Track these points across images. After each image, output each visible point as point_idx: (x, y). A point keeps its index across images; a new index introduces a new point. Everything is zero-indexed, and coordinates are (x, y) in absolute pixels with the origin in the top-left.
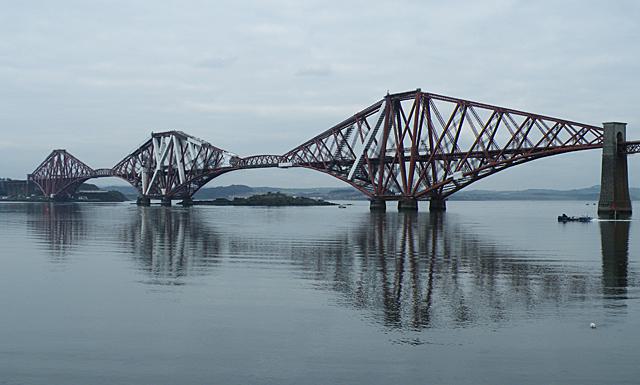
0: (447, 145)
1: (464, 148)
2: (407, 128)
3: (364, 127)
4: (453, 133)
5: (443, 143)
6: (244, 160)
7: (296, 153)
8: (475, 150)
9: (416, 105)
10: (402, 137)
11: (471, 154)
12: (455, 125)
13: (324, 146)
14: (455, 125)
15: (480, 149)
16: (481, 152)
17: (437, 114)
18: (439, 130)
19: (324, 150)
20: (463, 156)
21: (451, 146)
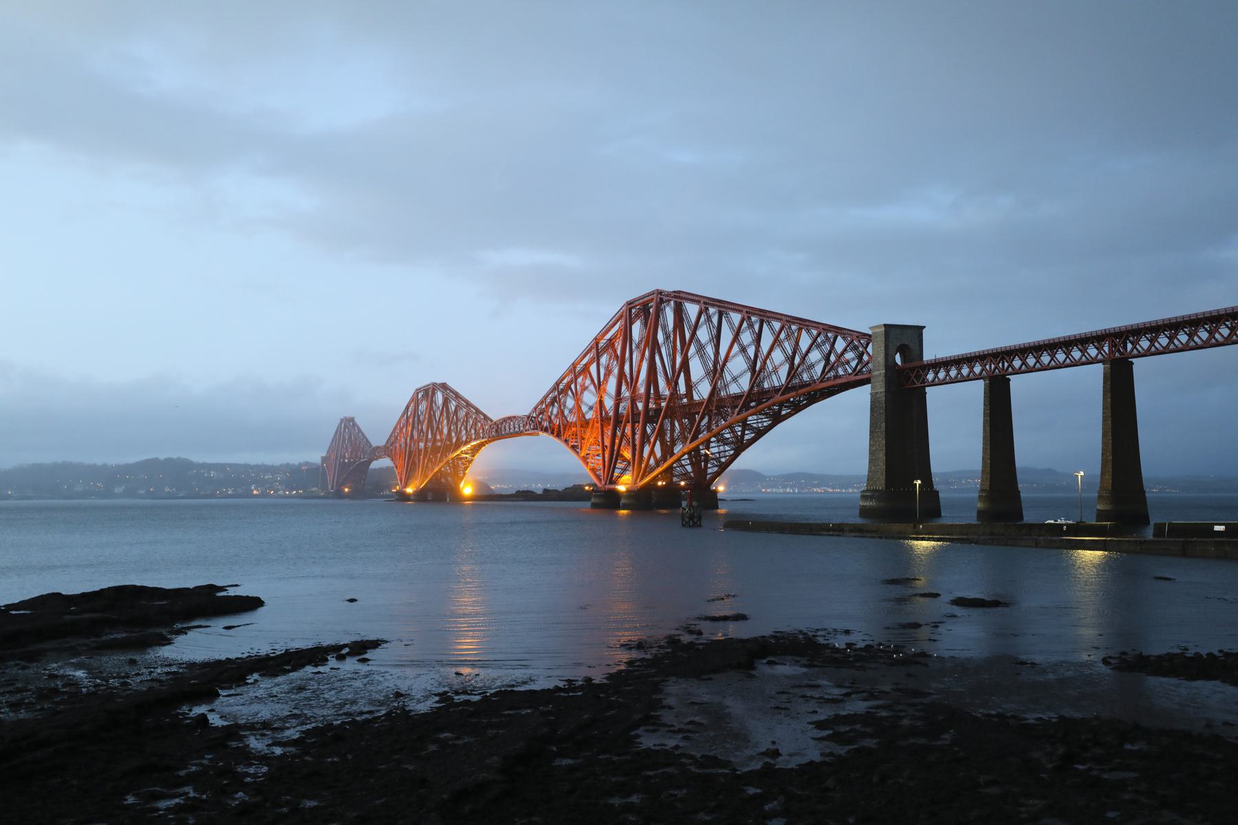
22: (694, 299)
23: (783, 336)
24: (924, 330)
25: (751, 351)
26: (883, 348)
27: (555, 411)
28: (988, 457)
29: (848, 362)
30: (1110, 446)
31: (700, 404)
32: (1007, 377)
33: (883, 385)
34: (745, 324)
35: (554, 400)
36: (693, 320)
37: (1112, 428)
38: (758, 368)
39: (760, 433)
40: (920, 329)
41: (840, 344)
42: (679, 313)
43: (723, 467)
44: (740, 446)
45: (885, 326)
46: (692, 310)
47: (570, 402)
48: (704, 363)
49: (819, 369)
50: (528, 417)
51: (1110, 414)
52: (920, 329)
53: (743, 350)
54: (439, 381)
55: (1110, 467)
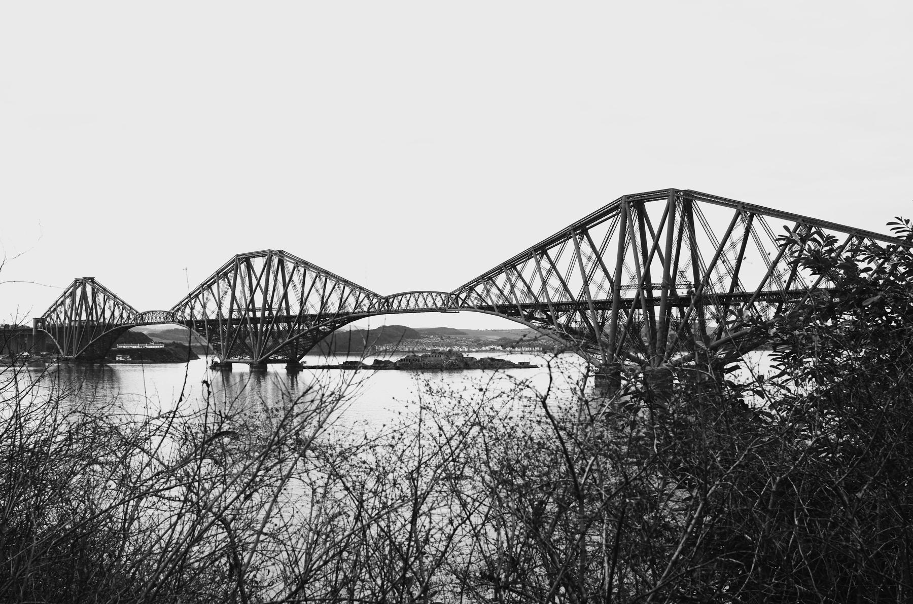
0: (720, 279)
1: (750, 282)
2: (656, 246)
3: (585, 247)
4: (731, 256)
5: (713, 277)
6: (387, 299)
7: (472, 289)
8: (765, 289)
9: (670, 211)
10: (647, 260)
11: (759, 295)
12: (733, 245)
13: (520, 276)
14: (733, 245)
15: (774, 288)
16: (775, 293)
17: (705, 225)
18: (707, 254)
19: (520, 284)
20: (747, 298)
21: (728, 282)
22: (292, 258)
23: (336, 286)
25: (321, 292)
27: (188, 310)
29: (365, 305)
31: (295, 317)
34: (318, 279)
35: (187, 303)
36: (291, 270)
38: (325, 300)
41: (362, 296)
42: (281, 262)
46: (290, 266)
47: (198, 307)
48: (297, 294)
49: (353, 306)
53: (317, 291)
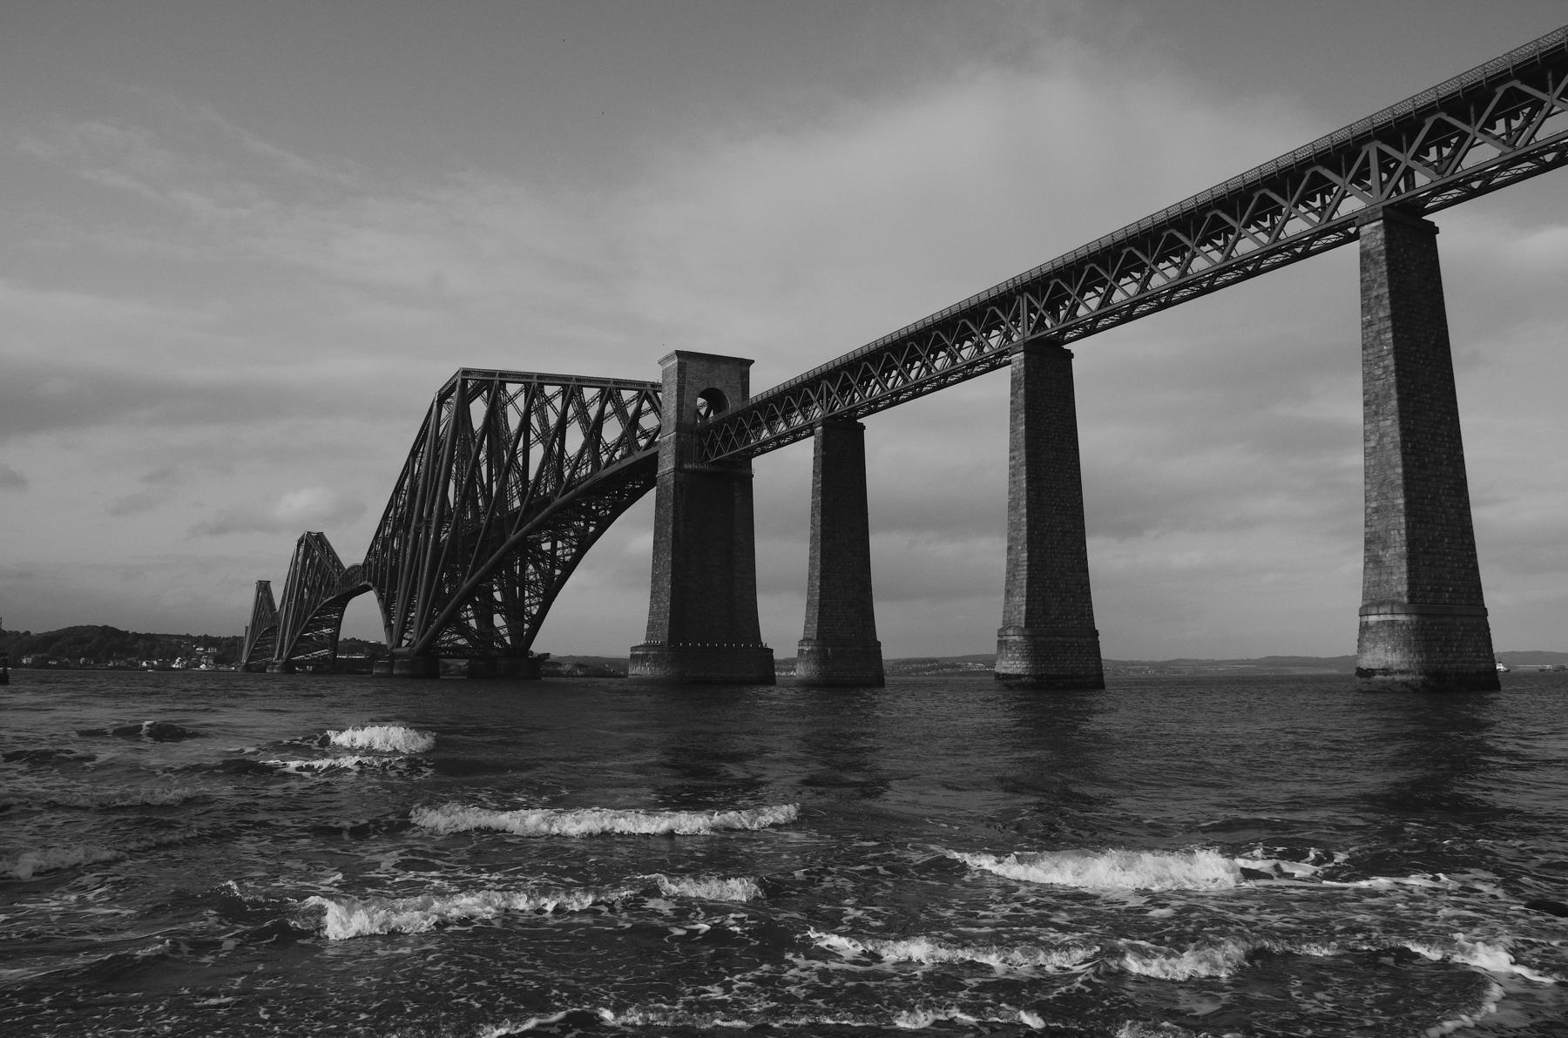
24: (752, 367)
26: (675, 394)
28: (817, 573)
30: (1024, 532)
32: (859, 421)
33: (673, 457)
37: (1028, 491)
39: (569, 569)
40: (742, 366)
43: (537, 621)
44: (551, 590)
45: (679, 353)
50: (367, 563)
51: (1023, 459)
52: (744, 365)
54: (315, 530)
55: (1023, 574)
